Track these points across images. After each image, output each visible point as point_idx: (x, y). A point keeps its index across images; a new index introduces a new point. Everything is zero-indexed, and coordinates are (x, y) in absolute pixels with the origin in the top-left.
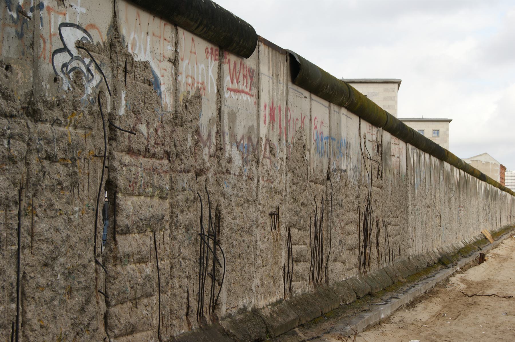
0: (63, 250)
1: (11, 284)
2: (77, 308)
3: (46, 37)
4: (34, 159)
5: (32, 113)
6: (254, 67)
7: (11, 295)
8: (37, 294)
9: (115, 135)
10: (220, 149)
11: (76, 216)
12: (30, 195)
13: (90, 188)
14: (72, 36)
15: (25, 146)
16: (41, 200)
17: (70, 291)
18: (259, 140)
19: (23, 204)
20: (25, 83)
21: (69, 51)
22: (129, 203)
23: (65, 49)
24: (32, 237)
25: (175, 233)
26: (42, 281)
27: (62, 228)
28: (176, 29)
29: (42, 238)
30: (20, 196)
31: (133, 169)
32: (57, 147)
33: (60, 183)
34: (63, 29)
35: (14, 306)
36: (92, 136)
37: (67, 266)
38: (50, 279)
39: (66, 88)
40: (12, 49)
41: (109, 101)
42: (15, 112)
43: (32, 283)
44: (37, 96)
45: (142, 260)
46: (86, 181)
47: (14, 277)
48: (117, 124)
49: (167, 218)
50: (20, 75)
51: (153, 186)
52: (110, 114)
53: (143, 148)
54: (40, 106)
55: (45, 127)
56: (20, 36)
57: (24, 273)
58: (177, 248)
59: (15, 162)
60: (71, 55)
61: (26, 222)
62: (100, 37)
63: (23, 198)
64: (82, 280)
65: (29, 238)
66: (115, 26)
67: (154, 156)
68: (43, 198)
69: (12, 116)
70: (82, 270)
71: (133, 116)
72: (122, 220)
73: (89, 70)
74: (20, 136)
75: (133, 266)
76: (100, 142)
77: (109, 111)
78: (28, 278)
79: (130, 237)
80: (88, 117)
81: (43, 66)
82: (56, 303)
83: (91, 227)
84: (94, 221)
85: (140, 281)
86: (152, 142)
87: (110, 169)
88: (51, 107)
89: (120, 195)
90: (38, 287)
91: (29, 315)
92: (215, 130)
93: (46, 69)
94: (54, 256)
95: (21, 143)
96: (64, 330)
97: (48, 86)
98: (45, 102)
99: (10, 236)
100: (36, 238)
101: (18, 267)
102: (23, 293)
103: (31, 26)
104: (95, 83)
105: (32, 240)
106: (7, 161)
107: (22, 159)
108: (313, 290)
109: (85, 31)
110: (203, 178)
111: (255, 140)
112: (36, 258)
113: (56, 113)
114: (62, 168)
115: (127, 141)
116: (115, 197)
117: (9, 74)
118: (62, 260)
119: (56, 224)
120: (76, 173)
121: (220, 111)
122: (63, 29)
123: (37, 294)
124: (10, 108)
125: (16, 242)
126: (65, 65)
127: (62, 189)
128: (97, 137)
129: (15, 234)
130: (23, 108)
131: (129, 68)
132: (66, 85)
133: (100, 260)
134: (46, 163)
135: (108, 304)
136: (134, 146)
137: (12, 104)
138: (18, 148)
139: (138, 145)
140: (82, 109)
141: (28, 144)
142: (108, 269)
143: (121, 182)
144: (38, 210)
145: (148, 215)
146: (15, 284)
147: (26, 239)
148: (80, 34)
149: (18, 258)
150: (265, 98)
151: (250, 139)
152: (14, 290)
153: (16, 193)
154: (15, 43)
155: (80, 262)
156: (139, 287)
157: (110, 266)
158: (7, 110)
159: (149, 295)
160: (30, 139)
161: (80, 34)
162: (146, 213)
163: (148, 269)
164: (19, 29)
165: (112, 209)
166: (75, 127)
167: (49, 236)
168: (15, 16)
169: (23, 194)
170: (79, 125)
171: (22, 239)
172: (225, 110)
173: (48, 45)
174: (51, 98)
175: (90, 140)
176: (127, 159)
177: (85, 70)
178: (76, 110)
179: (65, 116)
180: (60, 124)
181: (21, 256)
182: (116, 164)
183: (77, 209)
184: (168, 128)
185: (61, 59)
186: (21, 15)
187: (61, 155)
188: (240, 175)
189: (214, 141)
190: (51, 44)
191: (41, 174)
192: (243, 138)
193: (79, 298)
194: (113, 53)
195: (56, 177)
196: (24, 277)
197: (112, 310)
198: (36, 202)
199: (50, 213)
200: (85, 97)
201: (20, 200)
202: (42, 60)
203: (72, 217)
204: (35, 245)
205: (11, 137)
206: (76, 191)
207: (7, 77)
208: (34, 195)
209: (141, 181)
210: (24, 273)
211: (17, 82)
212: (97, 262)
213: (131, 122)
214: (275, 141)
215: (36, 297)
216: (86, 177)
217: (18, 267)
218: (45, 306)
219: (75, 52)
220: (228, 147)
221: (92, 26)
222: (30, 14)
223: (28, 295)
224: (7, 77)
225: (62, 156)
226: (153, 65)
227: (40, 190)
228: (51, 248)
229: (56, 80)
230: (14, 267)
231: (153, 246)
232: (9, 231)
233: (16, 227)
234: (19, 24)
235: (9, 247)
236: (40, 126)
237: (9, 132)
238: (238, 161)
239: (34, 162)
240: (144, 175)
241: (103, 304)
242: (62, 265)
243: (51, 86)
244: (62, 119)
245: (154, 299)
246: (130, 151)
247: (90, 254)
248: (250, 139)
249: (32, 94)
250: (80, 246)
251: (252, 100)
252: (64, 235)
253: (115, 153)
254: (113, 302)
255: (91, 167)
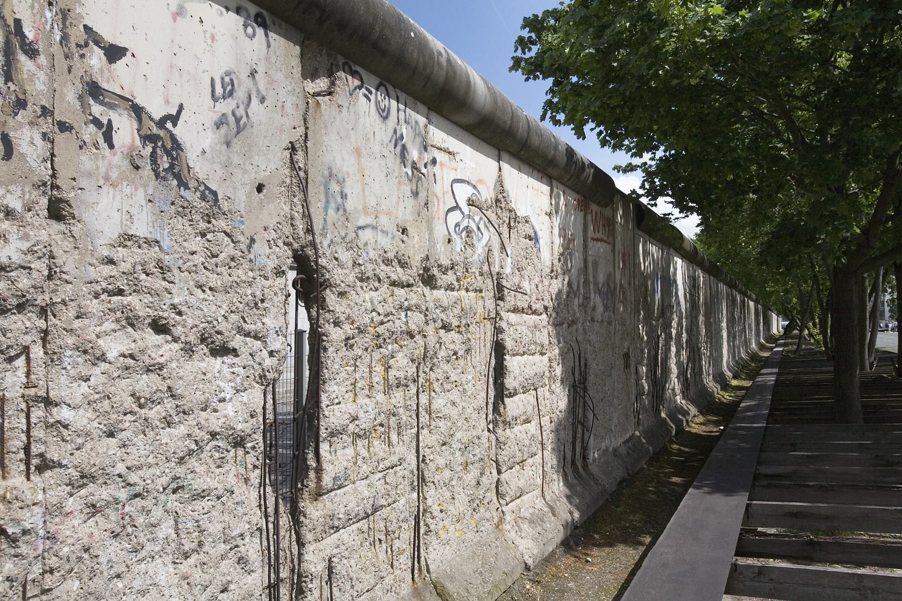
0: (460, 424)
1: (412, 472)
2: (474, 483)
3: (440, 195)
4: (430, 330)
5: (429, 280)
6: (611, 216)
7: (412, 484)
8: (437, 477)
9: (503, 295)
10: (587, 298)
11: (470, 385)
12: (427, 370)
13: (482, 356)
14: (463, 193)
15: (422, 316)
16: (438, 374)
17: (466, 465)
18: (615, 285)
19: (421, 380)
20: (421, 247)
21: (460, 210)
22: (515, 363)
23: (457, 207)
24: (430, 414)
25: (553, 387)
26: (441, 462)
27: (458, 401)
28: (551, 182)
29: (439, 415)
30: (418, 372)
31: (519, 328)
32: (452, 314)
33: (455, 353)
34: (455, 185)
35: (415, 495)
36: (482, 297)
37: (463, 441)
38: (448, 458)
39: (459, 250)
40: (408, 210)
41: (497, 259)
42: (412, 281)
43: (432, 466)
44: (432, 260)
45: (527, 421)
46: (478, 346)
47: (415, 462)
48: (504, 283)
49: (547, 374)
50: (416, 238)
51: (535, 343)
52: (498, 274)
53: (526, 306)
54: (435, 271)
55: (439, 294)
56: (416, 194)
57: (424, 456)
58: (555, 402)
59: (412, 337)
60: (463, 213)
61: (424, 399)
62: (487, 194)
63: (421, 374)
64: (477, 452)
65: (427, 417)
66: (500, 182)
67: (535, 312)
68: (439, 371)
69: (409, 286)
70: (477, 441)
71: (518, 273)
72: (510, 382)
73: (479, 229)
74: (418, 307)
75: (520, 427)
76: (490, 304)
77: (497, 270)
78: (428, 461)
79: (516, 398)
80: (479, 278)
81: (437, 228)
82: (454, 483)
83: (484, 394)
84: (485, 387)
85: (527, 442)
86: (534, 299)
87: (498, 330)
88: (444, 270)
89: (507, 357)
90: (438, 469)
91: (429, 502)
92: (582, 280)
93: (440, 232)
94: (452, 432)
95: (418, 314)
96: (462, 509)
97: (443, 248)
98: (440, 266)
99: (409, 419)
100: (434, 415)
101: (418, 451)
102: (424, 480)
103: (425, 185)
104: (484, 241)
105: (430, 418)
106: (405, 336)
107: (419, 332)
108: (654, 419)
109: (475, 187)
110: (575, 327)
111: (612, 286)
112: (434, 437)
113: (450, 277)
114: (457, 335)
115: (513, 299)
116: (503, 360)
117: (405, 238)
118: (458, 435)
119: (452, 398)
120: (469, 339)
121: (585, 261)
122: (455, 185)
123: (437, 477)
124: (407, 277)
125: (416, 424)
126: (457, 225)
127: (457, 359)
128: (486, 298)
129: (414, 417)
130: (419, 275)
131: (512, 224)
132: (458, 244)
133: (491, 426)
134: (442, 331)
135: (499, 472)
136: (519, 304)
137: (409, 272)
138: (415, 320)
139: (522, 303)
140: (474, 270)
141: (426, 315)
142: (498, 435)
143: (509, 344)
144: (436, 386)
145: (532, 373)
146: (416, 472)
147: (424, 418)
148: (470, 191)
149: (418, 440)
150: (619, 246)
151: (608, 284)
152: (415, 478)
153: (414, 370)
154: (410, 202)
155: (474, 434)
156: (526, 449)
157: (499, 431)
158: (404, 278)
159: (533, 455)
160: (427, 309)
161: (470, 191)
162: (530, 372)
163: (532, 428)
164: (414, 188)
165: (500, 371)
166: (467, 290)
167: (447, 412)
168: (410, 173)
169: (421, 371)
170: (471, 288)
171: (421, 419)
172: (590, 259)
173: (441, 204)
174: (446, 262)
175: (480, 303)
176: (513, 317)
177: (475, 229)
178: (467, 272)
179: (458, 280)
180: (453, 290)
181: (421, 438)
182: (503, 325)
183: (470, 377)
184: (546, 282)
185: (455, 217)
186: (415, 171)
187: (455, 323)
188: (602, 321)
189: (582, 291)
190: (444, 202)
191: (438, 345)
192: (603, 286)
193: (474, 471)
194: (499, 209)
195: (452, 346)
196: (423, 461)
197: (503, 476)
198: (433, 376)
199: (447, 386)
200: (476, 257)
201: (418, 376)
202: (436, 220)
203: (466, 387)
204: (433, 423)
205: (408, 309)
206: (469, 358)
207: (403, 241)
208: (431, 369)
209: (526, 340)
210: (424, 456)
211: (414, 247)
212: (489, 430)
213: (516, 280)
214: (626, 286)
215: (436, 481)
216: (478, 342)
217: (418, 451)
218: (444, 488)
219: (466, 209)
220: (592, 295)
221: (480, 181)
222: (424, 171)
223: (428, 479)
224: (403, 241)
225: (457, 324)
226: (533, 219)
227: (437, 363)
228: (449, 424)
229: (449, 241)
230: (414, 451)
231: (535, 403)
232: (408, 413)
233: (415, 408)
234: (414, 181)
235: (409, 431)
236: (435, 292)
237: (406, 303)
238: (600, 309)
239: (431, 333)
240: (528, 333)
241: (494, 472)
242: (459, 441)
243: (445, 248)
244: (456, 283)
245: (538, 458)
246: (516, 310)
247: (483, 423)
248: (608, 284)
249: (427, 258)
250: (475, 416)
251: (609, 247)
252: (460, 408)
253: (503, 313)
254: (503, 470)
255: (482, 331)
